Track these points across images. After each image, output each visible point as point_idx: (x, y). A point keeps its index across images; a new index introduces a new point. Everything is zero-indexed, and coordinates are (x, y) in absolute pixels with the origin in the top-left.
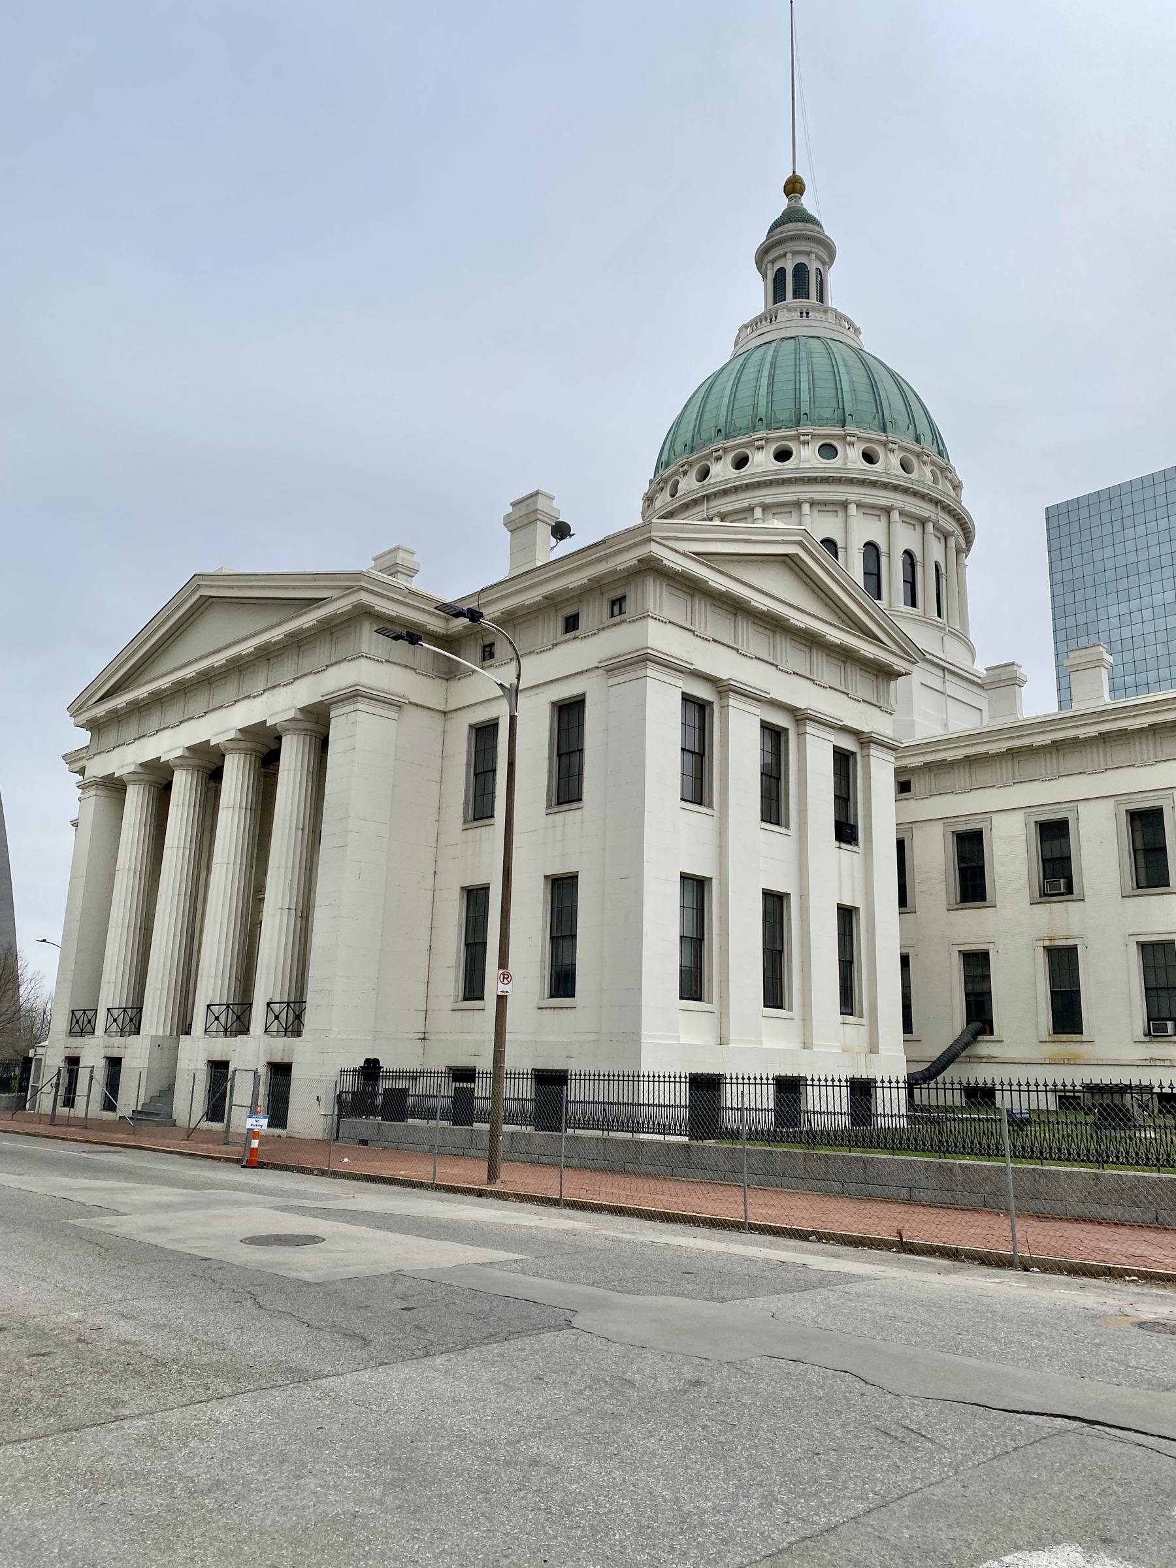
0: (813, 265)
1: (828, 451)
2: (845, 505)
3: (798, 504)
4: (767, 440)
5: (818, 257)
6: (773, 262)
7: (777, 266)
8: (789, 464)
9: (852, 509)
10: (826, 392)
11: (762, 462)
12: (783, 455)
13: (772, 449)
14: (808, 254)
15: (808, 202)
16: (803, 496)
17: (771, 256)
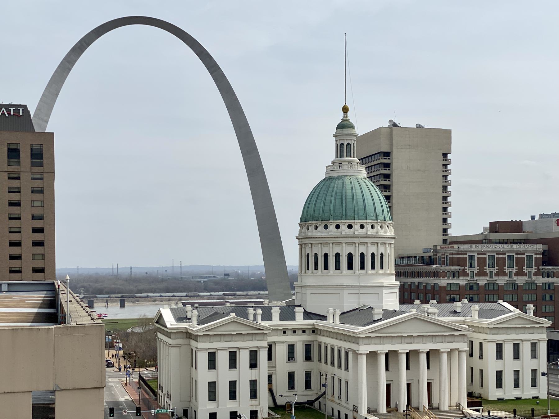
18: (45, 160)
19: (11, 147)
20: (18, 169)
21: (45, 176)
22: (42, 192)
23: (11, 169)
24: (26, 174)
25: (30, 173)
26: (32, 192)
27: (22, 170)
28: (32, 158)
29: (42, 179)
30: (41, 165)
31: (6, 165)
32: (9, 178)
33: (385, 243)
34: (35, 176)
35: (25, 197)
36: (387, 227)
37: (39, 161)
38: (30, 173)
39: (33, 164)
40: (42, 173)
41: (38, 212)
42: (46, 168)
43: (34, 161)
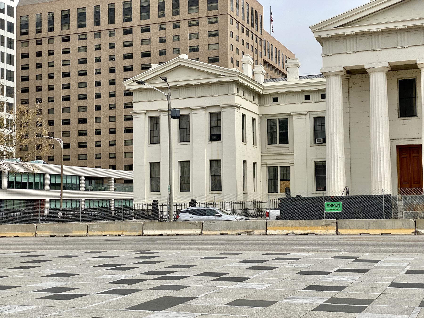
20: (196, 15)
23: (191, 16)
24: (204, 19)
25: (207, 18)
26: (209, 36)
27: (200, 16)
28: (208, 3)
30: (216, 8)
31: (187, 13)
32: (190, 26)
34: (211, 20)
35: (204, 41)
37: (215, 4)
38: (207, 18)
39: (209, 9)
40: (216, 17)
41: (213, 54)
42: (221, 10)
43: (210, 5)
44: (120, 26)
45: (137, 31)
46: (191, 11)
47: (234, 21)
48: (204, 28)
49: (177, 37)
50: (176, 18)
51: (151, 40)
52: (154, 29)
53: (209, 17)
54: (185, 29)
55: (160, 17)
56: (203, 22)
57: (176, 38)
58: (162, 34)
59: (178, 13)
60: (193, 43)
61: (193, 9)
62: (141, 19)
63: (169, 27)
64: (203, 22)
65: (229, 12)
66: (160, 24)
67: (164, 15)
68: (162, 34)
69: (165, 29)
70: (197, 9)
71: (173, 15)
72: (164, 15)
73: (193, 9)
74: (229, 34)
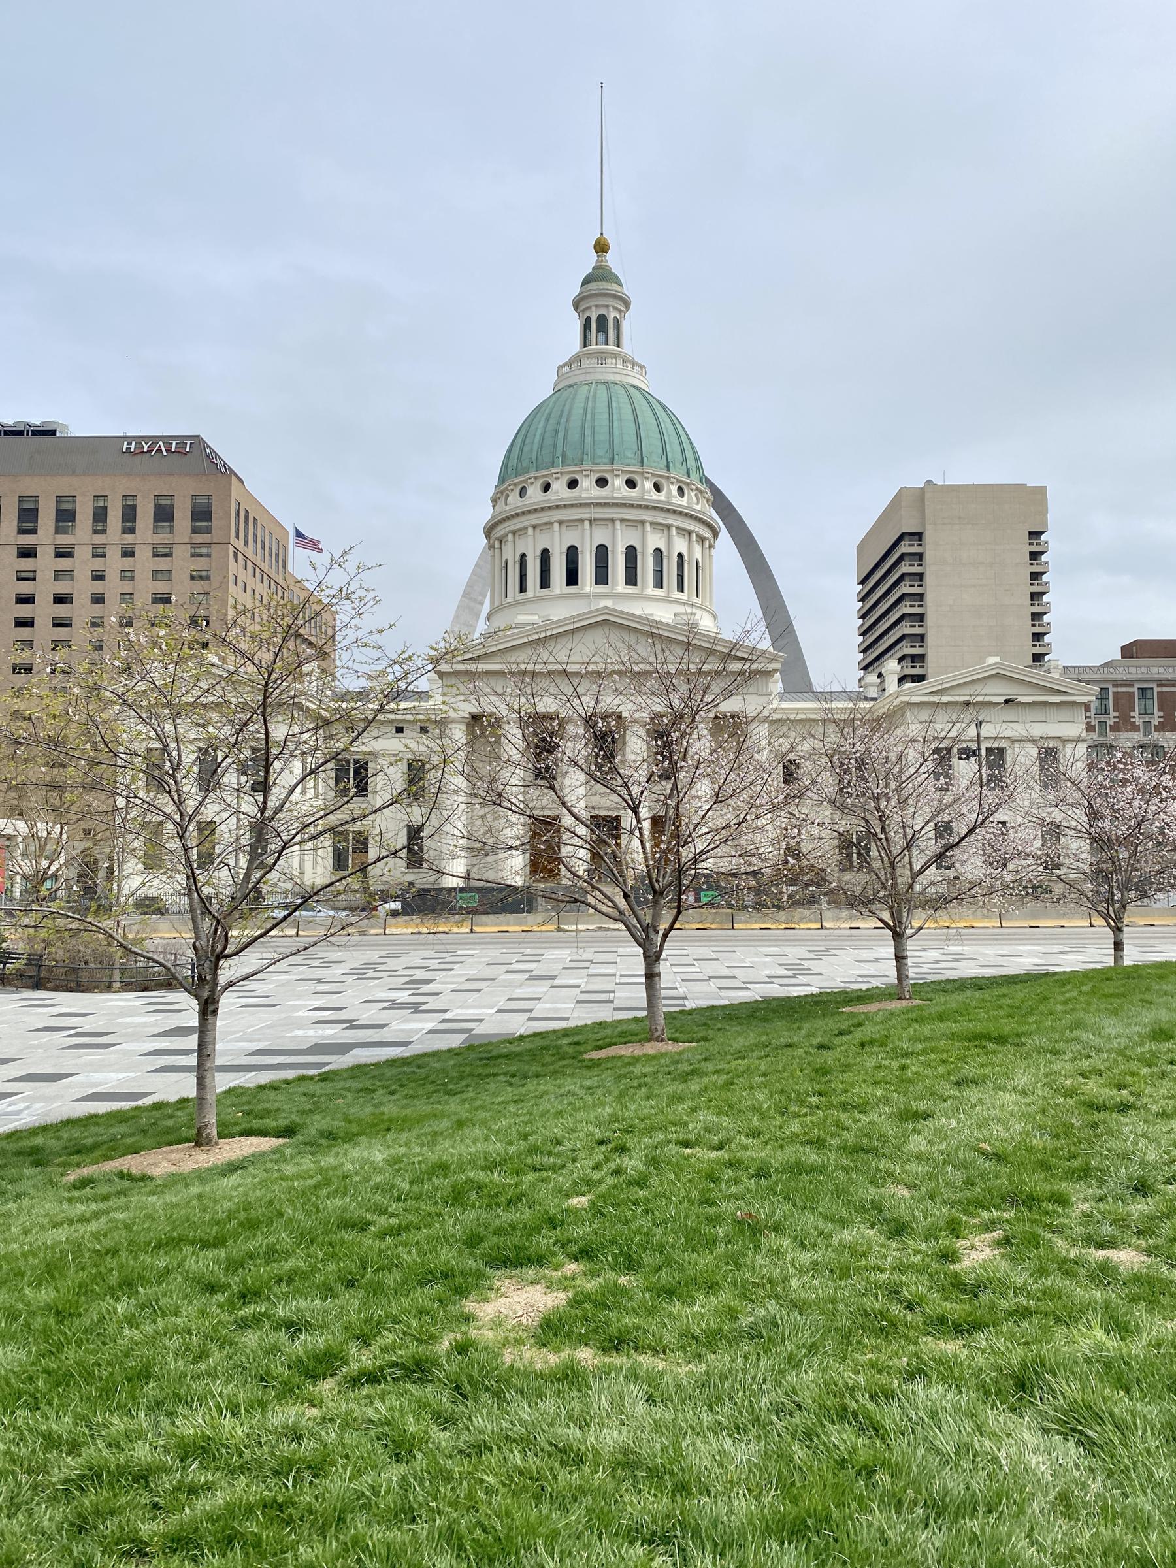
0: (612, 314)
1: (602, 482)
2: (613, 520)
3: (582, 521)
4: (562, 473)
5: (614, 308)
6: (583, 311)
7: (587, 314)
8: (575, 492)
9: (618, 523)
10: (603, 436)
11: (559, 489)
12: (573, 484)
13: (565, 480)
14: (607, 306)
15: (612, 260)
16: (584, 516)
17: (581, 308)
18: (214, 523)
19: (162, 502)
21: (214, 550)
22: (208, 578)
23: (158, 539)
26: (193, 578)
28: (193, 520)
29: (209, 556)
30: (208, 530)
33: (690, 533)
34: (197, 550)
35: (181, 589)
36: (693, 494)
39: (194, 531)
40: (208, 545)
42: (216, 535)
44: (12, 540)
45: (46, 556)
46: (160, 530)
47: (240, 556)
48: (182, 563)
49: (128, 574)
50: (129, 538)
51: (75, 573)
52: (83, 553)
53: (194, 545)
54: (144, 561)
55: (96, 532)
56: (182, 553)
57: (127, 576)
58: (98, 564)
59: (132, 531)
60: (161, 587)
61: (163, 527)
62: (57, 532)
63: (114, 553)
64: (182, 553)
65: (233, 540)
66: (95, 546)
67: (104, 531)
68: (98, 564)
69: (104, 556)
70: (172, 527)
71: (124, 532)
72: (104, 531)
73: (163, 527)
74: (231, 578)
